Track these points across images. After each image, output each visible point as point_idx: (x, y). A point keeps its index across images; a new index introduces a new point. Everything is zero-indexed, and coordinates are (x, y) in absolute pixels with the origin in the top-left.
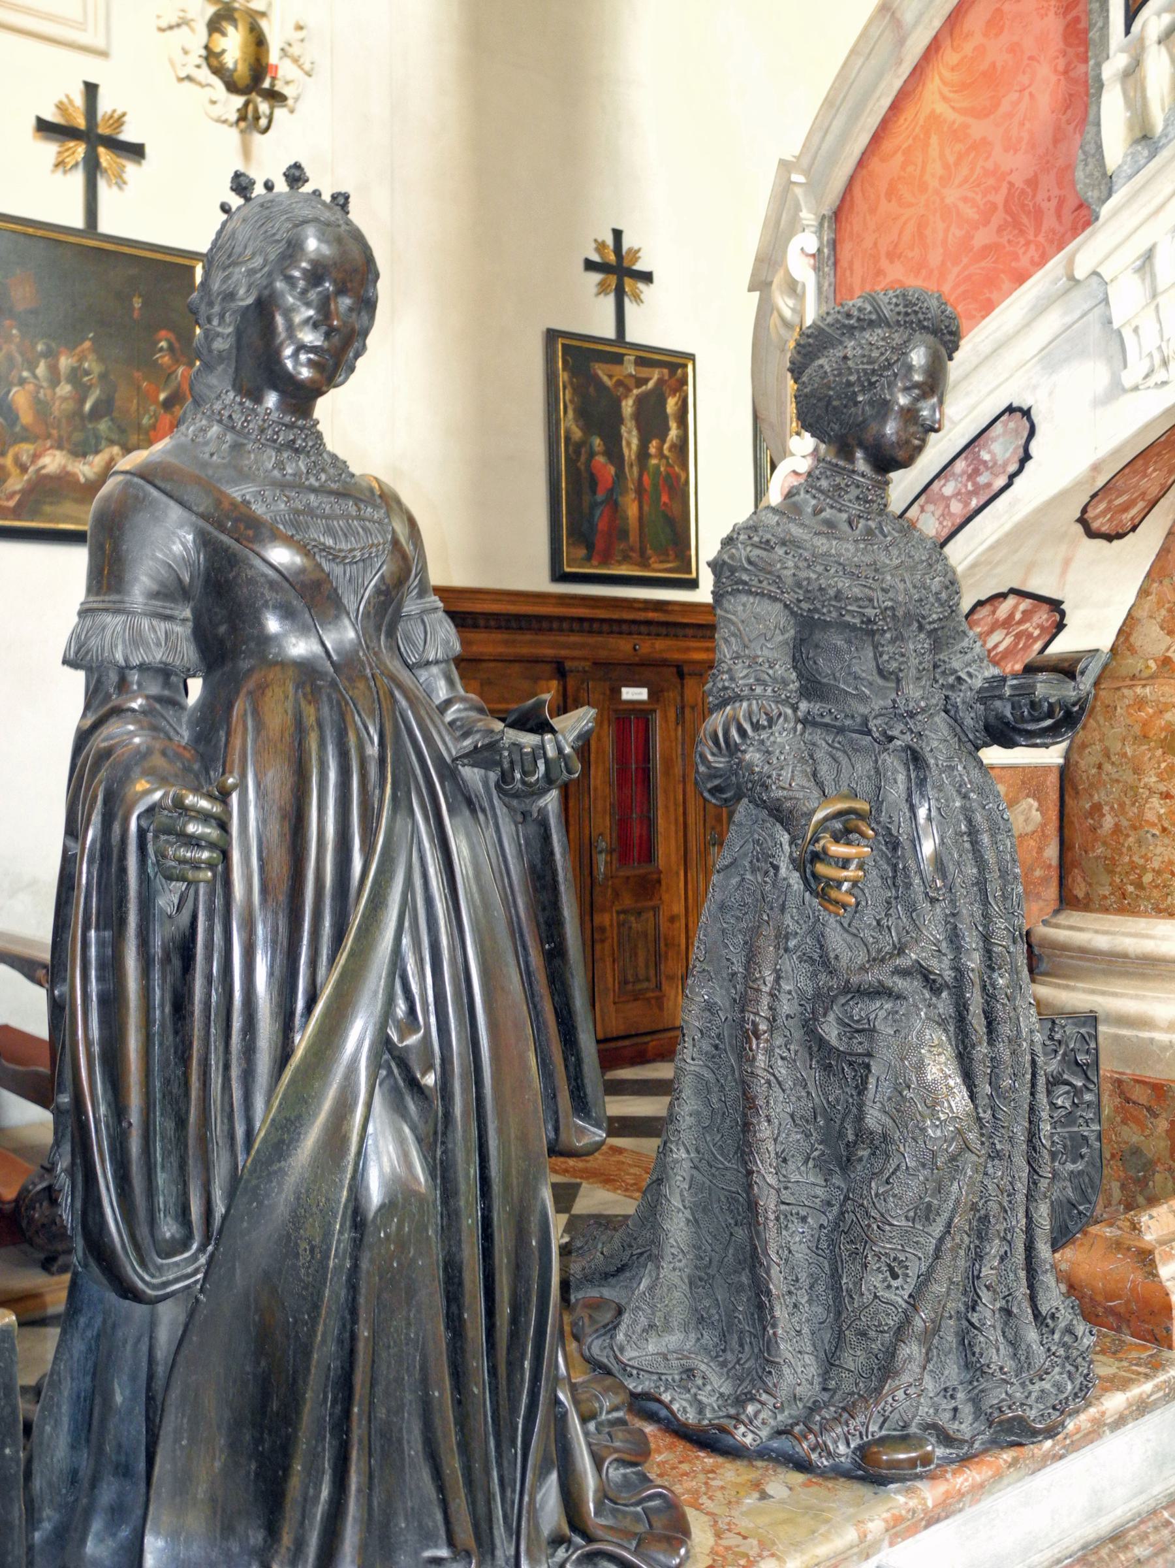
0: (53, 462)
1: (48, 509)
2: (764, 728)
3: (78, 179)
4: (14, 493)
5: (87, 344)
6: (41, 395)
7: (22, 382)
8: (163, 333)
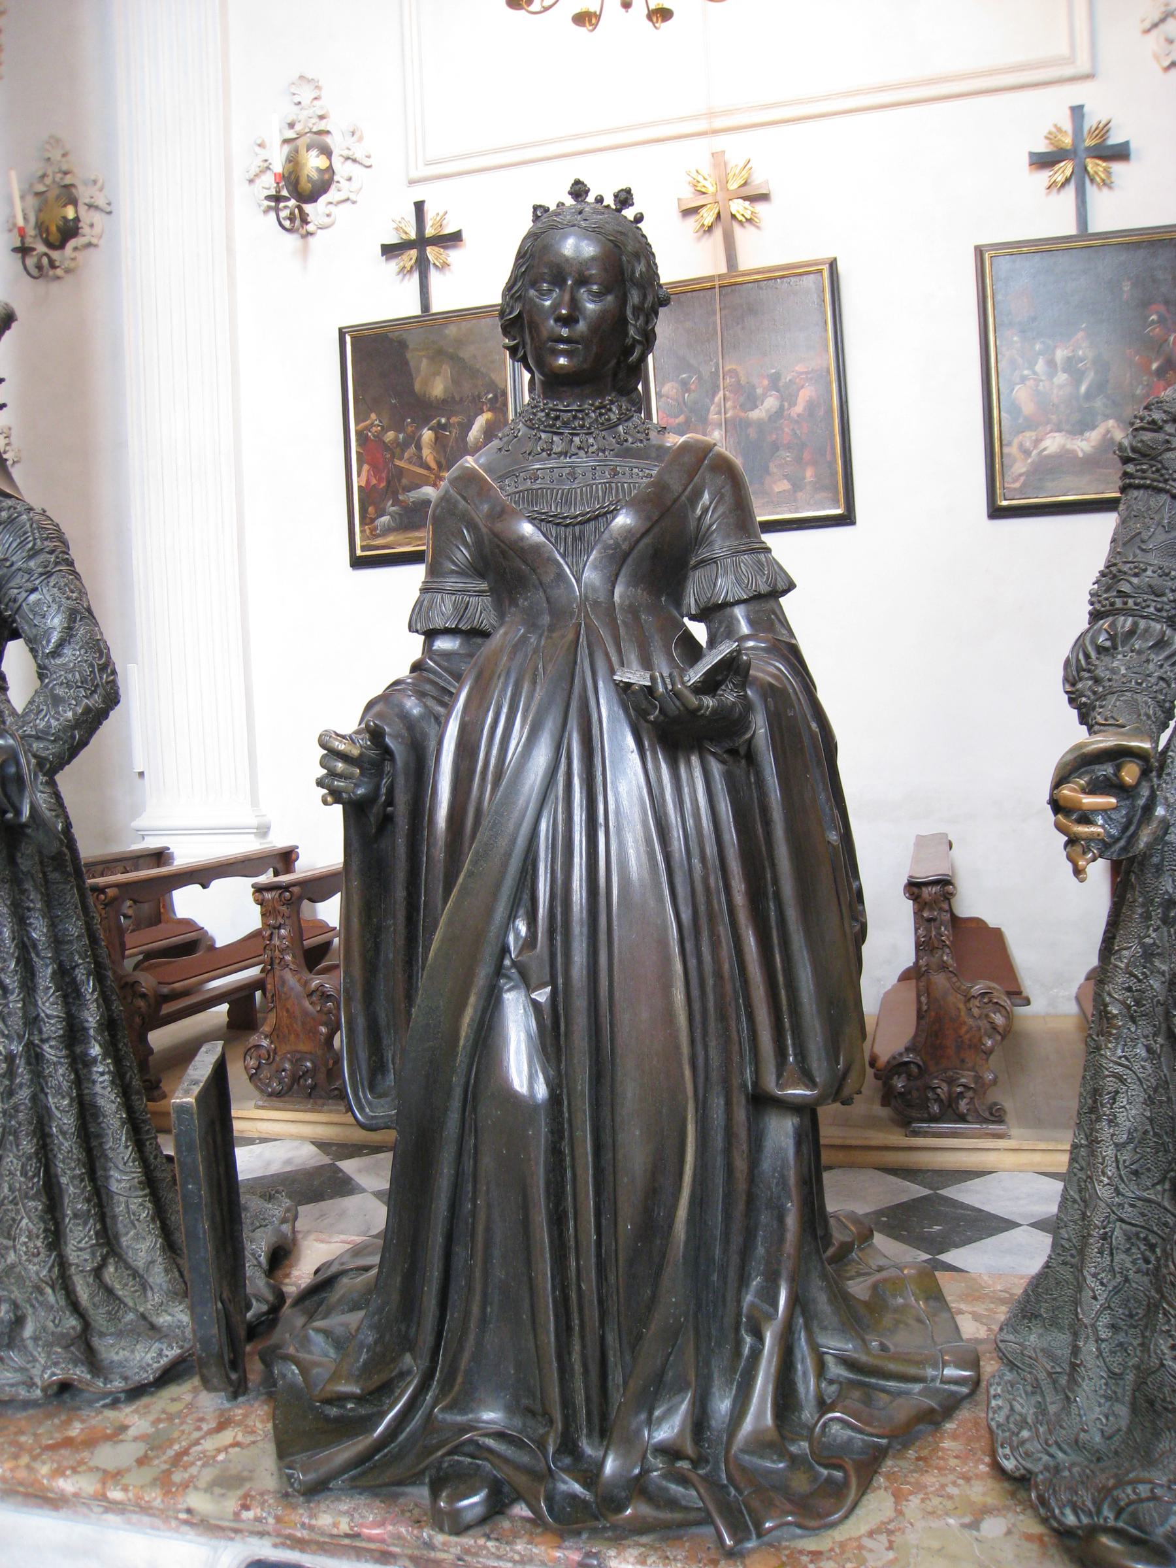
0: (1053, 443)
1: (1049, 485)
2: (1106, 649)
3: (1070, 192)
4: (1021, 475)
5: (1080, 335)
6: (1041, 388)
7: (1023, 380)
8: (1154, 307)
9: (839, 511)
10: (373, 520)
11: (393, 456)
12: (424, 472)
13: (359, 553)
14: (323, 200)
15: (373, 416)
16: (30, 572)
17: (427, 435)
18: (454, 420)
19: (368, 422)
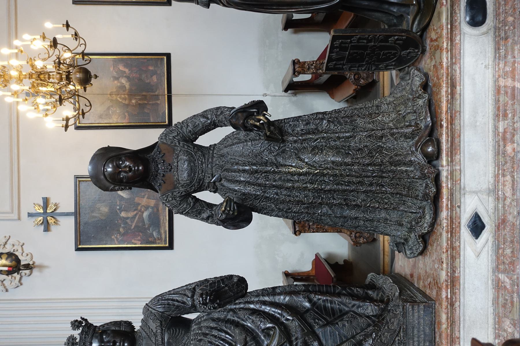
9: (165, 58)
10: (155, 239)
11: (130, 229)
12: (137, 217)
13: (167, 245)
14: (20, 257)
15: (113, 237)
16: (182, 127)
17: (123, 214)
18: (118, 203)
19: (115, 239)
